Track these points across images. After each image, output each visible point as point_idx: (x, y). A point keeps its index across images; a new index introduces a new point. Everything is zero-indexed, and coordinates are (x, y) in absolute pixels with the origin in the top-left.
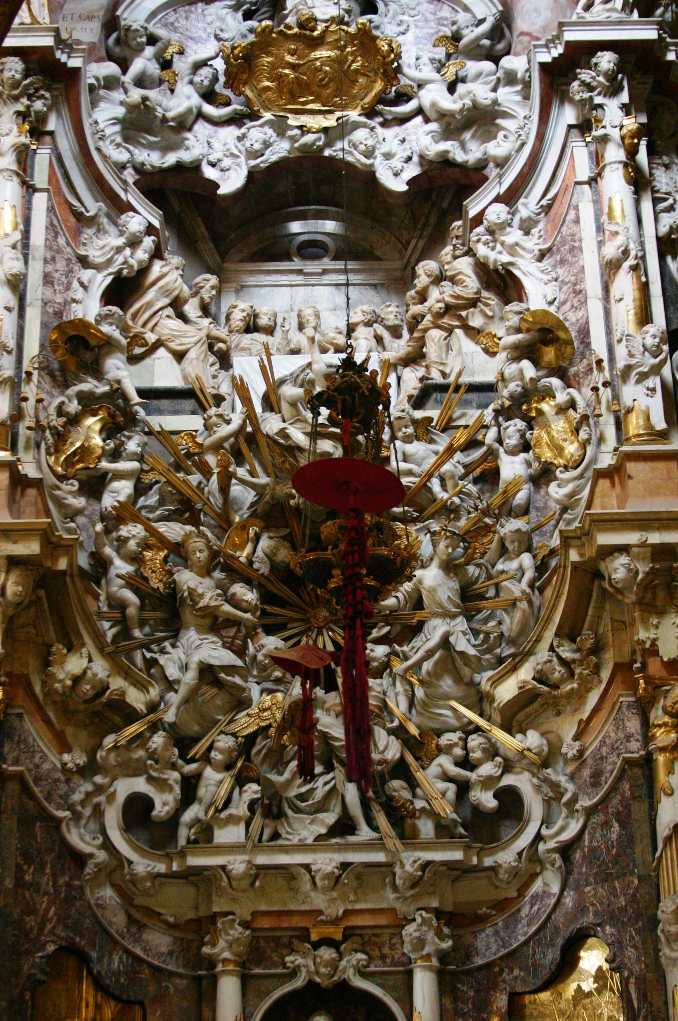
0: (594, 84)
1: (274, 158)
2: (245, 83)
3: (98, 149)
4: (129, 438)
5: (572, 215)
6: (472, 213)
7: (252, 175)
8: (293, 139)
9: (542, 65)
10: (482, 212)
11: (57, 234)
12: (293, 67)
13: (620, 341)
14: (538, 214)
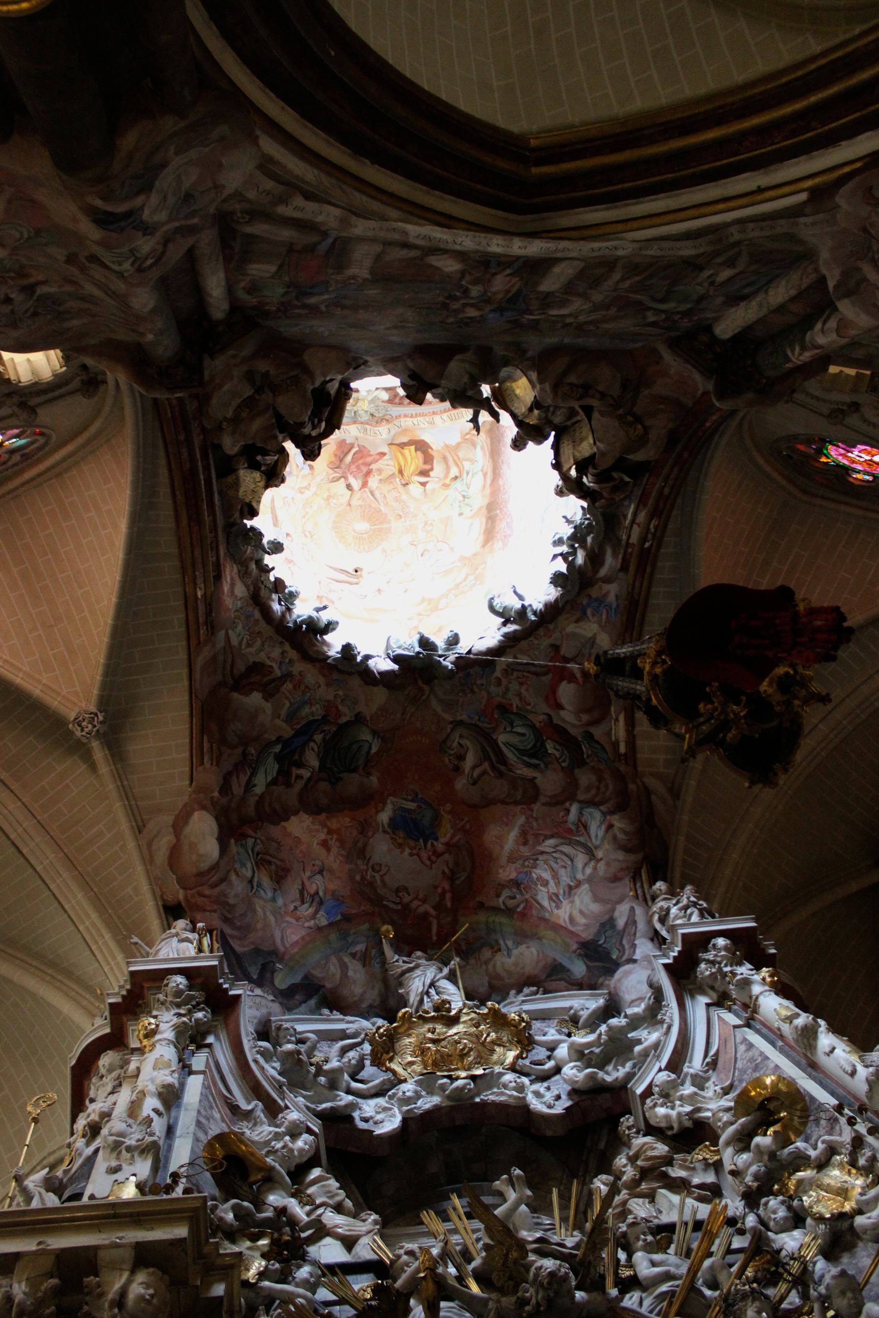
0: (719, 959)
1: (427, 1106)
2: (391, 1060)
3: (256, 1061)
4: (299, 1267)
5: (742, 1048)
6: (639, 1091)
7: (405, 1120)
8: (443, 1088)
9: (666, 966)
10: (650, 1086)
11: (211, 1108)
12: (434, 1041)
13: (853, 1073)
14: (706, 1072)
